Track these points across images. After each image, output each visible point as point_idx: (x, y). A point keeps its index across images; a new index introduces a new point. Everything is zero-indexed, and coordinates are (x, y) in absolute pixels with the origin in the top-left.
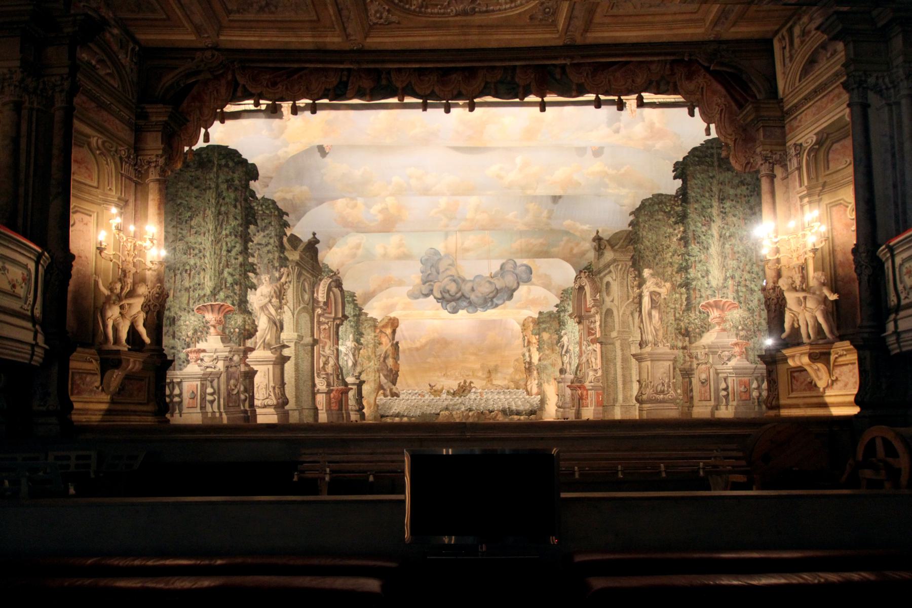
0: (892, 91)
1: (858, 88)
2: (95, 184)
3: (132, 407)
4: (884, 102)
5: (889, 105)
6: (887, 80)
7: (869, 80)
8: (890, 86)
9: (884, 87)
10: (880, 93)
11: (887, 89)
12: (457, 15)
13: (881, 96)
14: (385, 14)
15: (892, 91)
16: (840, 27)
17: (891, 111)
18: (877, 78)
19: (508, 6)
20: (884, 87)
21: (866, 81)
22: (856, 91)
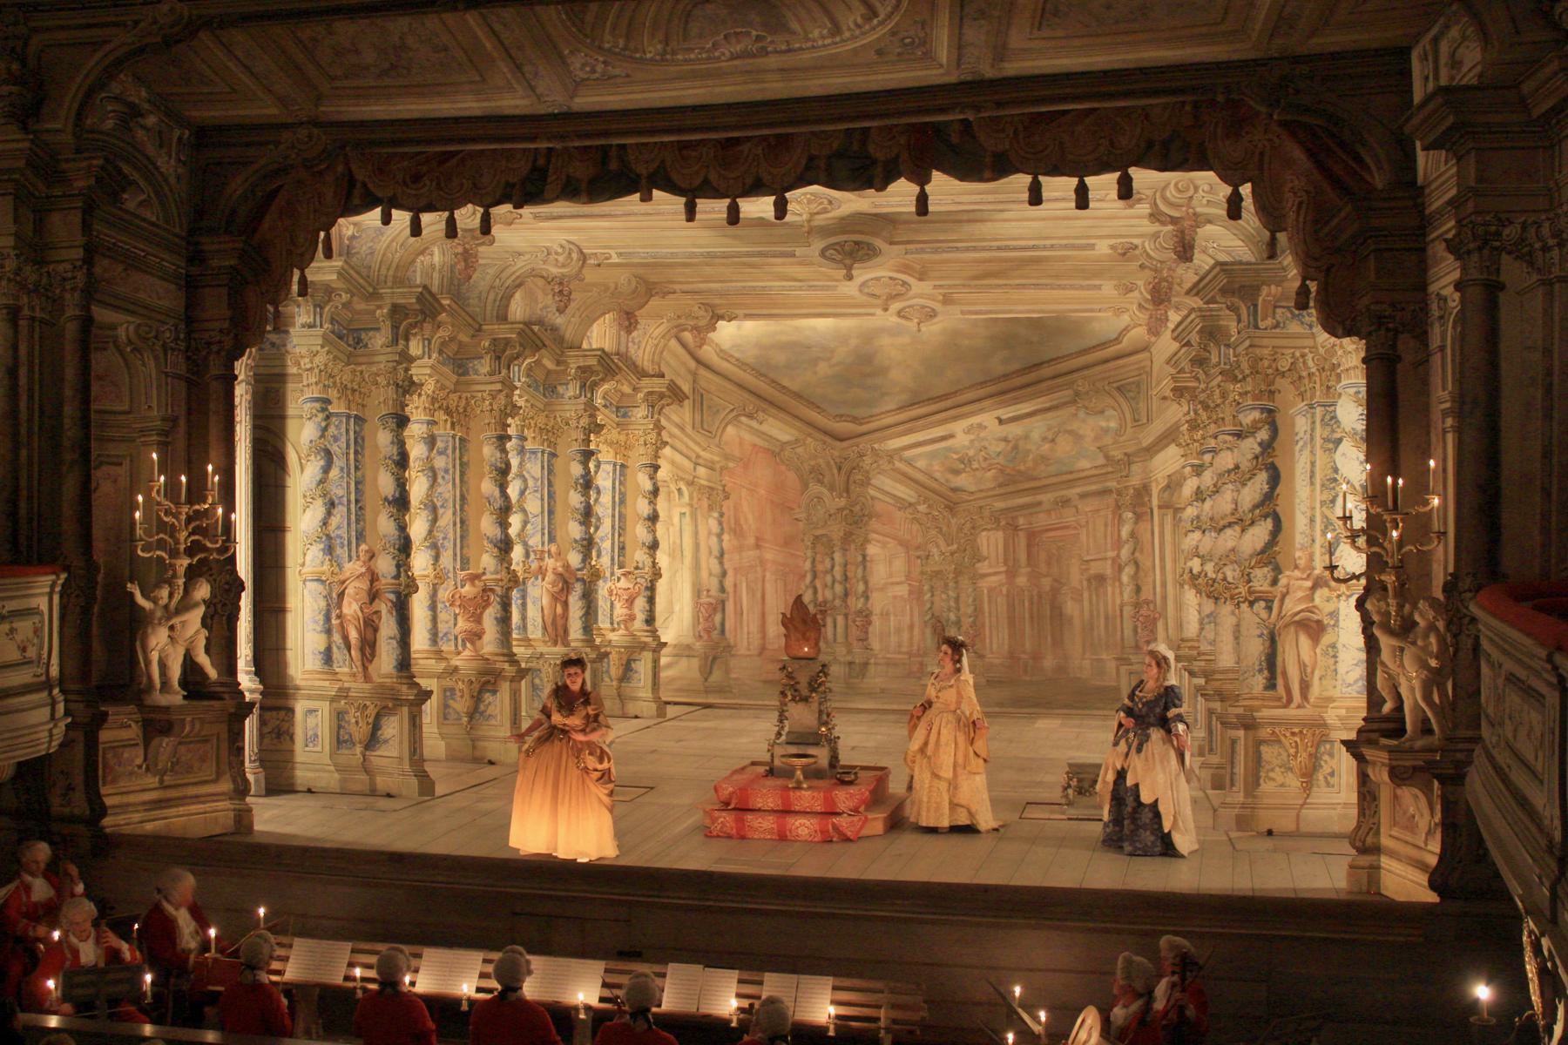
0: (1555, 252)
1: (1480, 249)
2: (126, 407)
3: (192, 791)
4: (1535, 277)
5: (1548, 283)
6: (1546, 230)
7: (1507, 231)
8: (1551, 242)
9: (1537, 246)
10: (1529, 259)
11: (1546, 249)
12: (732, 59)
13: (1531, 264)
14: (600, 68)
15: (1555, 252)
16: (1451, 119)
17: (1549, 296)
18: (1524, 227)
19: (828, 41)
20: (1537, 246)
21: (1498, 234)
22: (1475, 257)
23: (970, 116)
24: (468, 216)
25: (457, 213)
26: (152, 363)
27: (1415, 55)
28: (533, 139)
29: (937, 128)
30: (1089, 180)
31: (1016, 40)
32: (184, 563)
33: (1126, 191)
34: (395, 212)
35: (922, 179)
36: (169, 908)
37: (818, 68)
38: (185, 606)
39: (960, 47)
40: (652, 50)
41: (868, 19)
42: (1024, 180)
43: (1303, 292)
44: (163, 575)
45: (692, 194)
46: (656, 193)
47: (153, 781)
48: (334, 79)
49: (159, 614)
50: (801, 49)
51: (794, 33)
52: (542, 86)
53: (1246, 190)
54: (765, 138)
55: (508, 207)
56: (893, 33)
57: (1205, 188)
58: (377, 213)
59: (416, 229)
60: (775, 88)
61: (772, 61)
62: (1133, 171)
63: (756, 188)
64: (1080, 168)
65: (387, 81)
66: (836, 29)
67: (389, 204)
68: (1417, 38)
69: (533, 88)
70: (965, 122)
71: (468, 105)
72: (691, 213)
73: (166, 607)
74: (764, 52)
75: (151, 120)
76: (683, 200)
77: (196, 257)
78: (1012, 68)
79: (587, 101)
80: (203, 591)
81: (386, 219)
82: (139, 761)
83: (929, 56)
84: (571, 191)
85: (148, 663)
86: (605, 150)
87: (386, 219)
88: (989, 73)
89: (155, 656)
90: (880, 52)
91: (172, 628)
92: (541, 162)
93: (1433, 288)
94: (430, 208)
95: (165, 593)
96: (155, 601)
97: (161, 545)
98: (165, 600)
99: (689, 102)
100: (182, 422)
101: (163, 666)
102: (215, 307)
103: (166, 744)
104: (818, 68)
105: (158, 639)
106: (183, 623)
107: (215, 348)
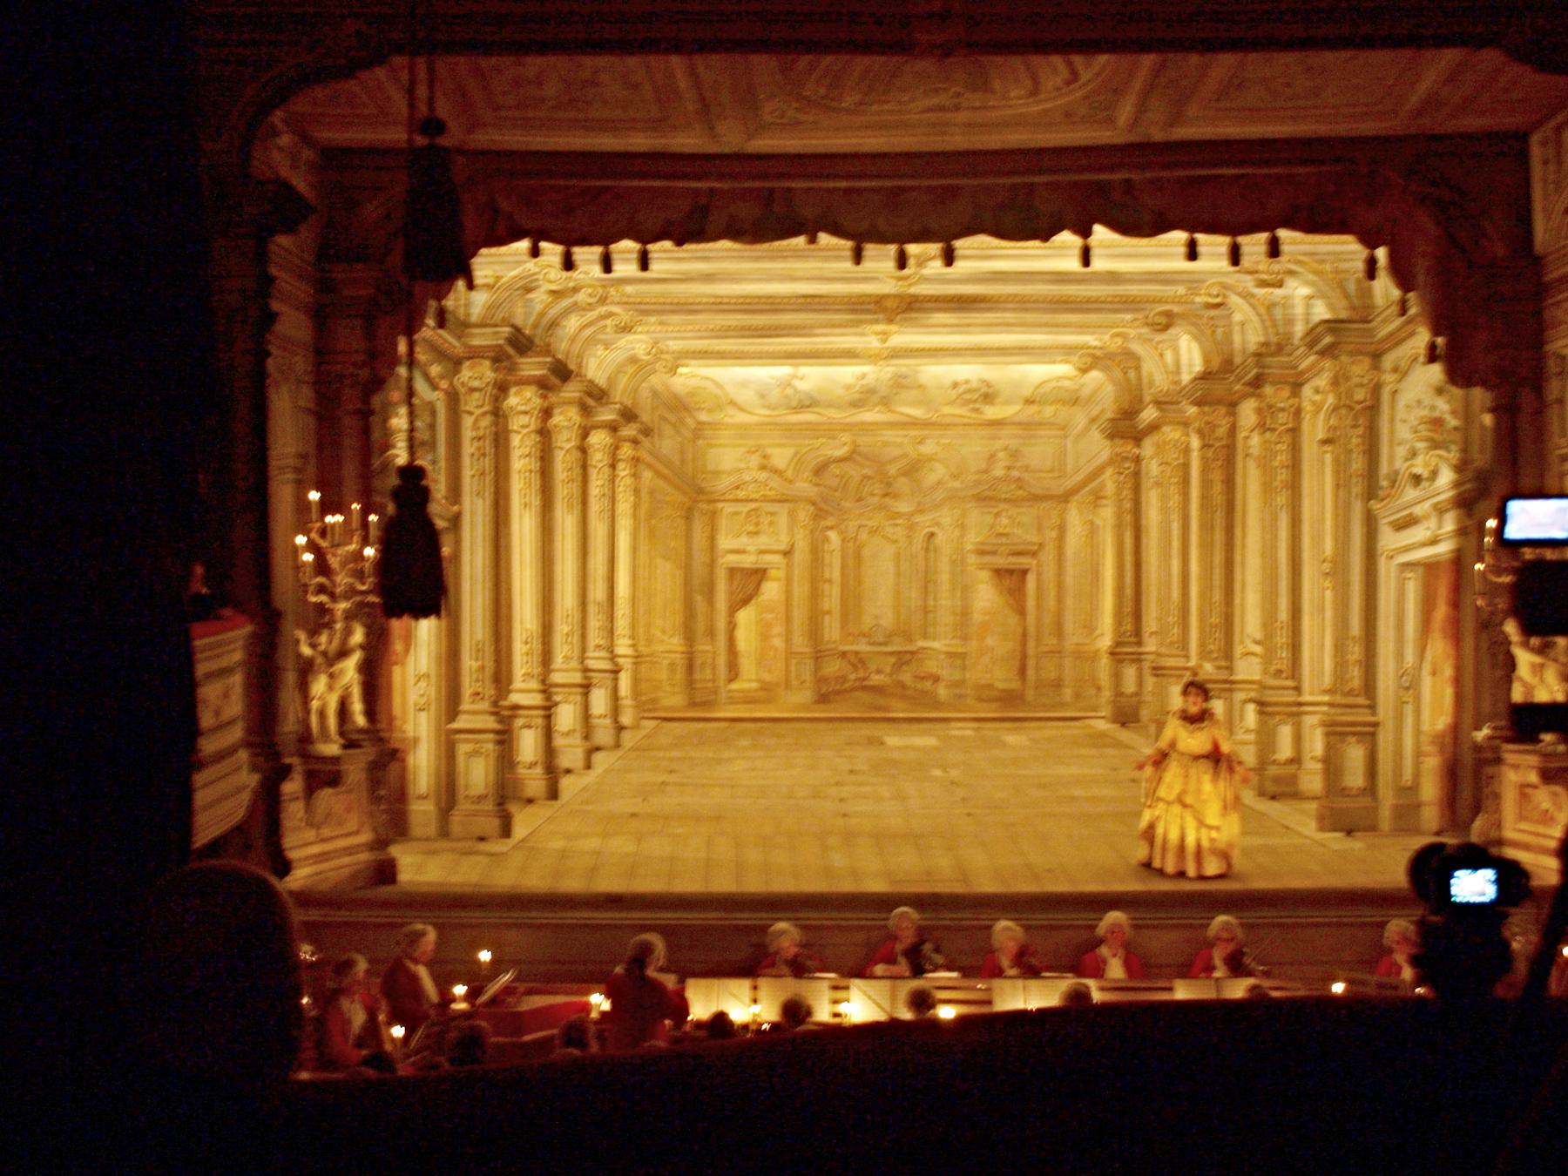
23: (1136, 176)
24: (626, 248)
25: (613, 247)
26: (286, 396)
27: (1535, 139)
28: (699, 178)
29: (1100, 187)
30: (1241, 239)
31: (1192, 110)
32: (342, 606)
33: (1274, 250)
34: (543, 245)
35: (1085, 233)
36: (412, 966)
37: (1005, 124)
38: (343, 653)
39: (1141, 109)
40: (849, 100)
41: (1068, 83)
42: (1179, 236)
43: (1432, 347)
44: (319, 619)
45: (860, 238)
46: (824, 238)
47: (310, 834)
48: (498, 108)
49: (319, 660)
50: (994, 107)
51: (993, 92)
52: (721, 128)
53: (1381, 253)
54: (930, 189)
55: (667, 244)
56: (1086, 98)
57: (1346, 249)
58: (524, 245)
59: (568, 264)
60: (958, 141)
61: (962, 117)
62: (1283, 234)
63: (922, 237)
64: (1233, 227)
65: (561, 114)
66: (1034, 92)
67: (538, 236)
68: (1540, 123)
69: (712, 128)
70: (1128, 181)
71: (639, 142)
72: (858, 257)
73: (324, 653)
74: (957, 108)
75: (285, 140)
76: (849, 244)
77: (324, 285)
78: (1182, 133)
79: (764, 144)
80: (358, 636)
81: (535, 252)
82: (301, 814)
83: (1110, 121)
84: (738, 231)
85: (307, 711)
86: (772, 191)
87: (535, 252)
88: (1158, 135)
89: (315, 704)
90: (1068, 115)
91: (331, 676)
92: (703, 201)
93: (1550, 348)
94: (585, 241)
95: (323, 638)
96: (313, 646)
97: (321, 589)
98: (322, 648)
99: (866, 149)
100: (313, 461)
101: (322, 714)
102: (349, 337)
103: (325, 795)
104: (1005, 124)
105: (319, 686)
106: (341, 671)
107: (347, 381)
